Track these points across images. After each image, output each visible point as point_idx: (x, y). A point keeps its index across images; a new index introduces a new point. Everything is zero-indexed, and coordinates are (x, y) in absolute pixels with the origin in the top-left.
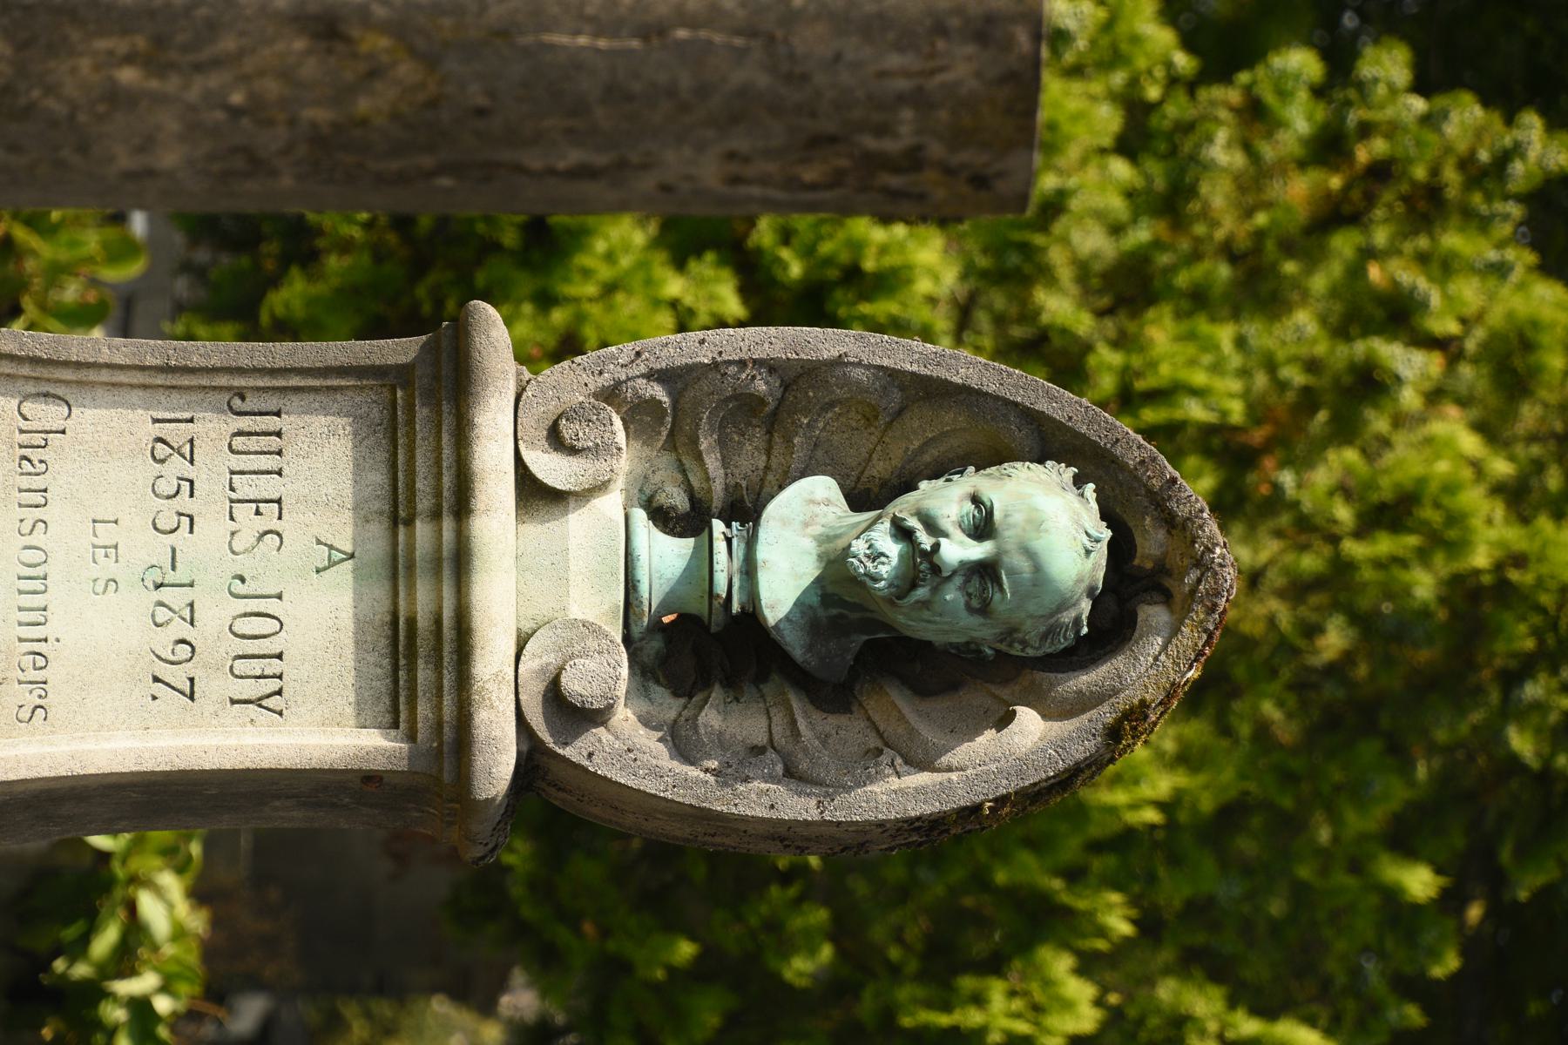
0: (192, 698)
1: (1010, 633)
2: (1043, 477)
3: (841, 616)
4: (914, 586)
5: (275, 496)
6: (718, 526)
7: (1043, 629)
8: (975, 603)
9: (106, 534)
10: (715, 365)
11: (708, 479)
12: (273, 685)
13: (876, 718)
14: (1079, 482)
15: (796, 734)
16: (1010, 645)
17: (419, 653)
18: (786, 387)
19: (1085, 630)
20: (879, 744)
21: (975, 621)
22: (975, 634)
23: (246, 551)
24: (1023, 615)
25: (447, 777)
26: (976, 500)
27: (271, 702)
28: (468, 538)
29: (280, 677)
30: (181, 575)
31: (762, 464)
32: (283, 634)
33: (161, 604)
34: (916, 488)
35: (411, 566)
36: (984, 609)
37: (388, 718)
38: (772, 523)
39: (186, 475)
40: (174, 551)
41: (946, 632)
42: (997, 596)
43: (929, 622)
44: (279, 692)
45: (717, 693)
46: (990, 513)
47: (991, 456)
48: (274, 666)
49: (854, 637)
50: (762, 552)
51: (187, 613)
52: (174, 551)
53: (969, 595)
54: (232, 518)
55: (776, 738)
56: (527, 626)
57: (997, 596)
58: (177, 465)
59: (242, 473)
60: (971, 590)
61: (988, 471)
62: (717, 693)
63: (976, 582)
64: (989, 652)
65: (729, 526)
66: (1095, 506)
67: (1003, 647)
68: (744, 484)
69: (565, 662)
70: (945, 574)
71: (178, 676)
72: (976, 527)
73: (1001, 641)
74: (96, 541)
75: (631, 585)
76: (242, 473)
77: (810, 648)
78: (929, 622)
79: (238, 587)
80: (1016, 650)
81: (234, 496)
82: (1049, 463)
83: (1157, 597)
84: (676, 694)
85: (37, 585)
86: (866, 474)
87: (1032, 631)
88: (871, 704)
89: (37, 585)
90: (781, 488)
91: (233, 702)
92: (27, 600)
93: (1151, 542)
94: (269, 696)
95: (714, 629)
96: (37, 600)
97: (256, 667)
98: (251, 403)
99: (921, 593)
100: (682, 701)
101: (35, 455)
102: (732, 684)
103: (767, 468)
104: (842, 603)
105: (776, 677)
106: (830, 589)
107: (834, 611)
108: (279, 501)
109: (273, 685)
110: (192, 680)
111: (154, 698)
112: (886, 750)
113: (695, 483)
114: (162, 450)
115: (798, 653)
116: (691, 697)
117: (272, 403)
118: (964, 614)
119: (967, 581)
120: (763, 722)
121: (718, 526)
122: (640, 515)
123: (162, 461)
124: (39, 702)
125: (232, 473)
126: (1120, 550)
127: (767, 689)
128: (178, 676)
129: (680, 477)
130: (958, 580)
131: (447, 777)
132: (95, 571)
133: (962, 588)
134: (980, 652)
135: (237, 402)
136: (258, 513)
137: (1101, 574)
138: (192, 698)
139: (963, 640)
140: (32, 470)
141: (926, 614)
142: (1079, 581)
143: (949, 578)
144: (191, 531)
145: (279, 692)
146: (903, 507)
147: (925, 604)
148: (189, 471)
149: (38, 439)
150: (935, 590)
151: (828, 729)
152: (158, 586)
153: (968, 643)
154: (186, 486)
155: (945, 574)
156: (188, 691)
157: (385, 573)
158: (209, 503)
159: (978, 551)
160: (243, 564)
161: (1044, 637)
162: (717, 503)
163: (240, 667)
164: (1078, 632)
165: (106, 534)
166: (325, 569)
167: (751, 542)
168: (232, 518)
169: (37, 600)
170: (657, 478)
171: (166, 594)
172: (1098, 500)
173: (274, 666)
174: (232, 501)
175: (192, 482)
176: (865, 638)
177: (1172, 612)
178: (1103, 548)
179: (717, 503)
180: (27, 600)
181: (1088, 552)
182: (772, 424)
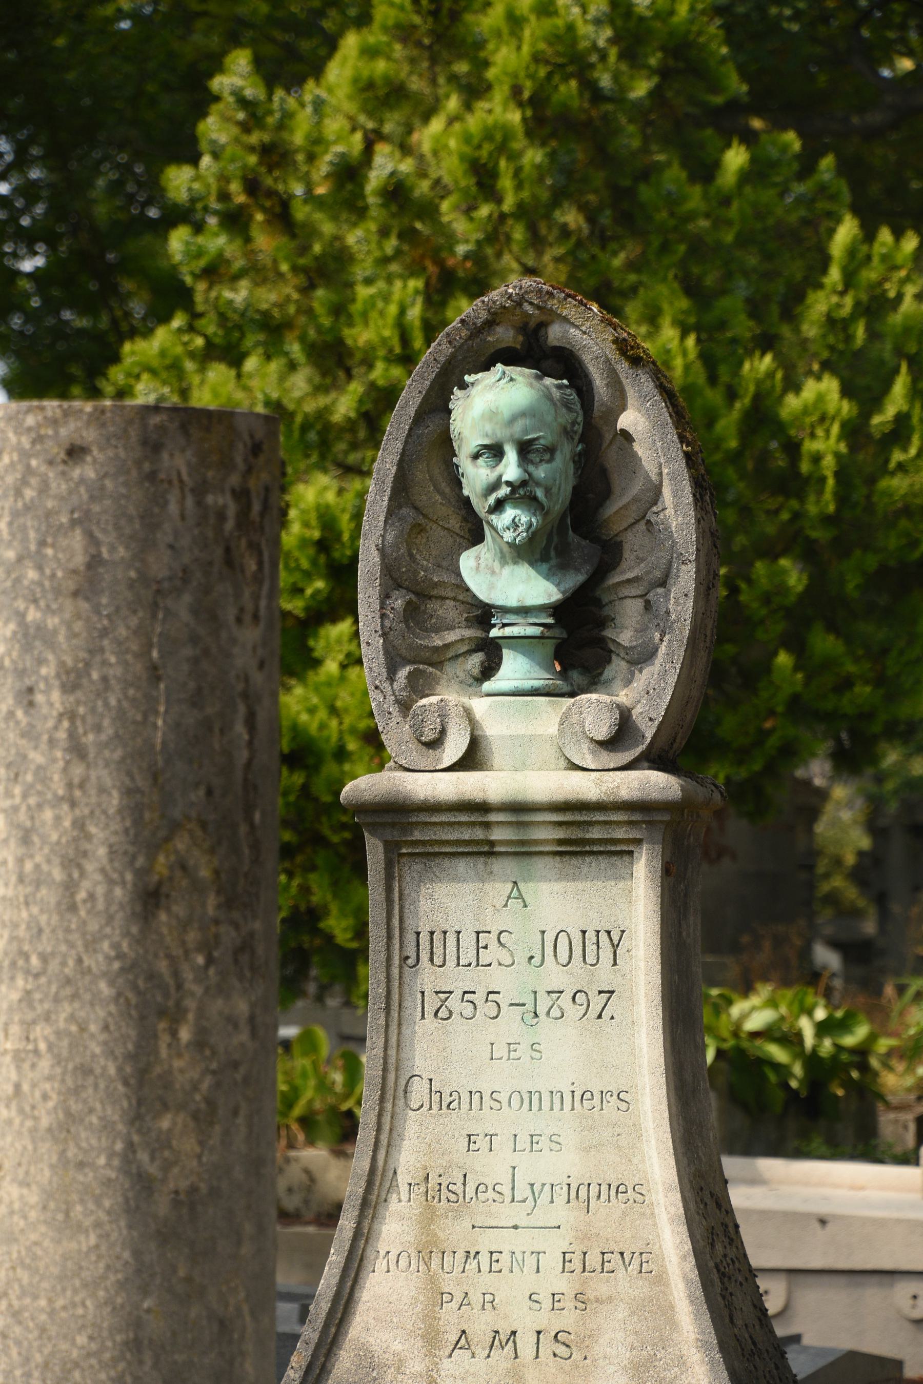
0: (612, 992)
1: (567, 432)
2: (460, 410)
3: (556, 548)
4: (535, 499)
5: (474, 935)
6: (494, 633)
7: (564, 410)
8: (547, 457)
9: (501, 1051)
10: (384, 635)
11: (462, 640)
13: (625, 525)
14: (463, 386)
15: (636, 579)
16: (576, 432)
17: (581, 836)
18: (399, 586)
19: (565, 382)
20: (643, 522)
21: (558, 456)
22: (568, 457)
23: (512, 955)
24: (555, 424)
25: (666, 817)
26: (476, 456)
28: (503, 804)
29: (598, 932)
31: (452, 603)
32: (568, 930)
33: (548, 1013)
34: (468, 497)
35: (522, 843)
36: (551, 450)
37: (626, 858)
38: (492, 596)
39: (460, 996)
40: (512, 1005)
41: (567, 476)
42: (542, 441)
44: (609, 932)
45: (609, 633)
46: (485, 447)
47: (445, 444)
49: (570, 540)
50: (512, 602)
51: (555, 996)
52: (512, 1005)
53: (541, 461)
54: (490, 965)
55: (639, 593)
56: (563, 763)
57: (542, 441)
59: (458, 958)
60: (538, 460)
61: (456, 448)
62: (609, 633)
63: (532, 456)
64: (580, 447)
65: (494, 626)
66: (480, 375)
67: (577, 438)
68: (465, 615)
69: (587, 737)
71: (597, 1002)
72: (495, 456)
73: (573, 439)
74: (505, 1058)
76: (458, 958)
77: (577, 570)
79: (537, 961)
80: (579, 428)
81: (474, 964)
82: (451, 406)
83: (542, 332)
84: (609, 661)
85: (535, 1098)
86: (458, 531)
87: (565, 418)
88: (616, 528)
89: (535, 1098)
90: (468, 590)
91: (615, 964)
92: (546, 1104)
93: (505, 336)
94: (611, 939)
95: (565, 635)
96: (546, 1097)
97: (591, 948)
98: (411, 951)
99: (540, 493)
100: (614, 657)
101: (446, 1100)
102: (603, 622)
103: (454, 599)
104: (546, 549)
105: (598, 593)
106: (538, 556)
107: (553, 553)
108: (478, 933)
109: (603, 937)
110: (600, 992)
111: (612, 1018)
112: (647, 518)
113: (465, 648)
114: (443, 1013)
115: (581, 578)
116: (611, 651)
117: (410, 937)
119: (532, 462)
120: (628, 602)
121: (494, 633)
122: (487, 686)
123: (451, 1012)
124: (615, 1097)
125: (458, 965)
126: (510, 357)
127: (605, 599)
128: (597, 1002)
129: (461, 659)
130: (531, 468)
131: (666, 817)
132: (526, 1059)
133: (536, 465)
134: (580, 454)
135: (411, 962)
136: (486, 947)
137: (527, 371)
138: (612, 992)
139: (572, 465)
140: (456, 1102)
141: (555, 490)
142: (531, 385)
143: (530, 475)
144: (498, 993)
145: (609, 932)
146: (481, 506)
147: (548, 491)
148: (457, 994)
149: (435, 1098)
150: (538, 484)
151: (633, 557)
153: (574, 462)
155: (527, 477)
157: (526, 861)
158: (479, 980)
159: (511, 455)
160: (521, 957)
161: (569, 409)
162: (479, 634)
163: (591, 959)
164: (567, 387)
165: (501, 1051)
166: (524, 901)
167: (505, 610)
168: (490, 965)
169: (546, 1097)
170: (462, 675)
171: (542, 1010)
172: (476, 373)
174: (478, 965)
175: (465, 992)
176: (570, 532)
177: (552, 322)
178: (509, 369)
179: (479, 634)
180: (546, 1104)
181: (512, 380)
182: (425, 596)
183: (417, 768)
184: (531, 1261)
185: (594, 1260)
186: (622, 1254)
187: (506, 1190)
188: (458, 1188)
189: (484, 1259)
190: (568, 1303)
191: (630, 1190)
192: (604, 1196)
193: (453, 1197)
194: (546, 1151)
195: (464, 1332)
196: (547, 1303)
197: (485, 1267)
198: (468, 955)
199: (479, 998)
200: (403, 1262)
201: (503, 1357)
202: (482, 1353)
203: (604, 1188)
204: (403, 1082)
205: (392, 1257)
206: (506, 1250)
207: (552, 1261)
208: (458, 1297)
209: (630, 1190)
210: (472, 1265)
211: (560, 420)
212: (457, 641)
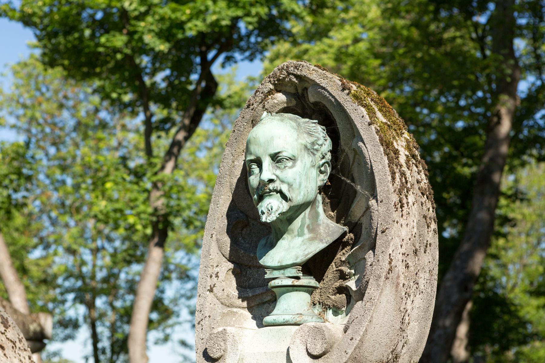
1: (310, 149)
3: (308, 227)
8: (290, 164)
21: (299, 163)
43: (300, 185)
49: (320, 222)
50: (275, 264)
53: (285, 167)
60: (283, 166)
70: (274, 177)
78: (300, 185)
99: (285, 188)
107: (306, 231)
118: (294, 169)
129: (266, 305)
130: (278, 172)
147: (290, 185)
150: (283, 182)
211: (300, 141)
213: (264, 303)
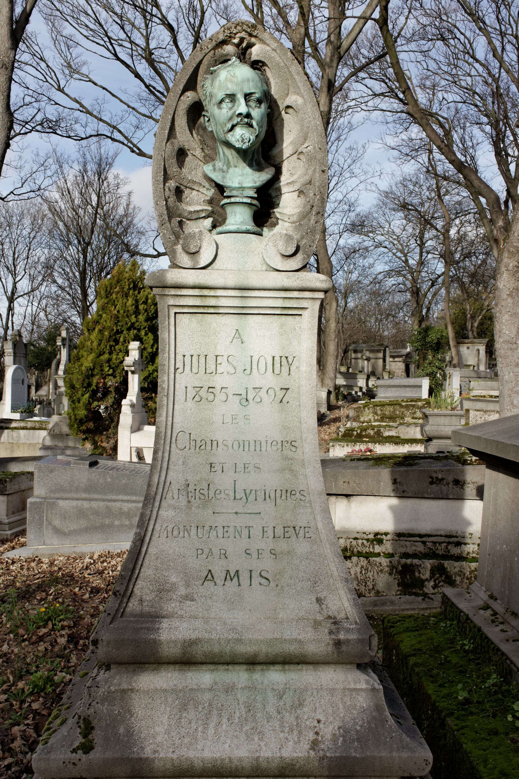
0: (288, 389)
5: (215, 357)
12: (284, 359)
23: (235, 368)
27: (290, 360)
30: (244, 393)
32: (266, 356)
48: (277, 359)
51: (257, 390)
55: (293, 190)
56: (264, 267)
58: (203, 393)
75: (248, 232)
84: (278, 224)
85: (246, 444)
92: (252, 448)
96: (252, 444)
98: (179, 365)
100: (280, 222)
101: (198, 444)
105: (270, 191)
107: (254, 164)
108: (217, 356)
109: (284, 360)
113: (203, 215)
114: (197, 398)
116: (278, 219)
117: (179, 357)
123: (201, 398)
124: (289, 444)
129: (201, 220)
135: (179, 371)
138: (288, 389)
140: (204, 446)
145: (287, 357)
149: (193, 443)
151: (289, 174)
152: (247, 400)
154: (210, 390)
156: (285, 391)
160: (240, 369)
163: (277, 371)
171: (250, 397)
173: (277, 359)
180: (252, 448)
183: (187, 267)
184: (245, 532)
185: (279, 531)
186: (294, 528)
187: (232, 494)
188: (205, 492)
189: (220, 531)
190: (266, 554)
191: (298, 494)
192: (284, 497)
193: (203, 497)
194: (252, 472)
195: (210, 571)
196: (255, 555)
197: (220, 535)
198: (211, 367)
199: (217, 391)
200: (175, 533)
201: (231, 586)
202: (220, 582)
203: (284, 491)
204: (174, 435)
205: (170, 529)
206: (232, 524)
207: (256, 532)
208: (206, 551)
209: (298, 494)
210: (213, 533)
212: (200, 211)
213: (200, 218)
